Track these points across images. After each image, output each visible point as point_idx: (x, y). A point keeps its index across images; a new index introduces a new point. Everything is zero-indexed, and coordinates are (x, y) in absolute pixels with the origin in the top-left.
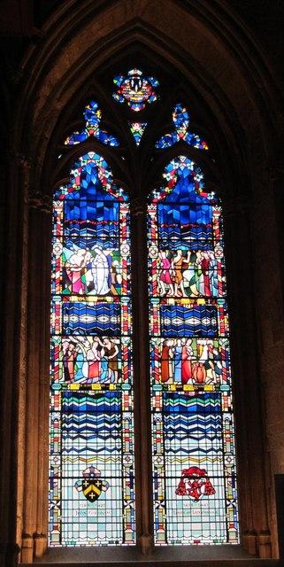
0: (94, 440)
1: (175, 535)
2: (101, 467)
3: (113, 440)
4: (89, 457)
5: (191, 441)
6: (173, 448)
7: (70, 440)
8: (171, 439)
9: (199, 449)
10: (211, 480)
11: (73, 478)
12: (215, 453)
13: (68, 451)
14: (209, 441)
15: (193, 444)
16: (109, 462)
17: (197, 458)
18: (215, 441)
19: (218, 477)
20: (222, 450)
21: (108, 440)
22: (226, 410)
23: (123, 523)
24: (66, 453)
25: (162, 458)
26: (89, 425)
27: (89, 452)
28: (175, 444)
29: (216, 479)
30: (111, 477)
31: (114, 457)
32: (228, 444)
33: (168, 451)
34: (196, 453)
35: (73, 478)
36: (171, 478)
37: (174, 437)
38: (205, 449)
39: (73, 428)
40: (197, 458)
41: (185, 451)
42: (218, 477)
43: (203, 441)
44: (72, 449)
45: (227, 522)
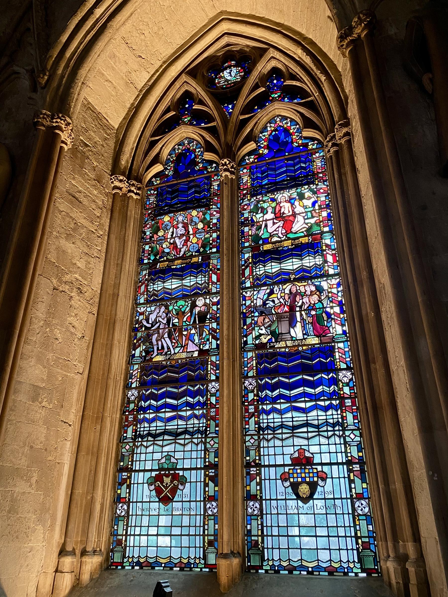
0: (175, 422)
1: (276, 558)
2: (179, 455)
3: (196, 421)
4: (165, 443)
5: (295, 414)
6: (272, 425)
7: (146, 425)
8: (268, 413)
9: (307, 424)
10: (326, 469)
11: (145, 471)
12: (329, 428)
13: (142, 437)
14: (321, 413)
15: (300, 417)
16: (188, 448)
17: (305, 435)
18: (329, 412)
19: (337, 464)
20: (342, 425)
21: (191, 422)
22: (344, 366)
23: (204, 535)
24: (140, 440)
25: (256, 437)
26: (169, 401)
27: (166, 437)
28: (275, 419)
29: (335, 467)
30: (191, 469)
31: (195, 441)
32: (350, 417)
33: (263, 429)
34: (305, 429)
35: (145, 471)
36: (269, 466)
37: (274, 410)
38: (316, 422)
39: (150, 407)
40: (305, 435)
41: (287, 427)
42: (337, 464)
43: (314, 413)
44: (149, 434)
45: (357, 538)
